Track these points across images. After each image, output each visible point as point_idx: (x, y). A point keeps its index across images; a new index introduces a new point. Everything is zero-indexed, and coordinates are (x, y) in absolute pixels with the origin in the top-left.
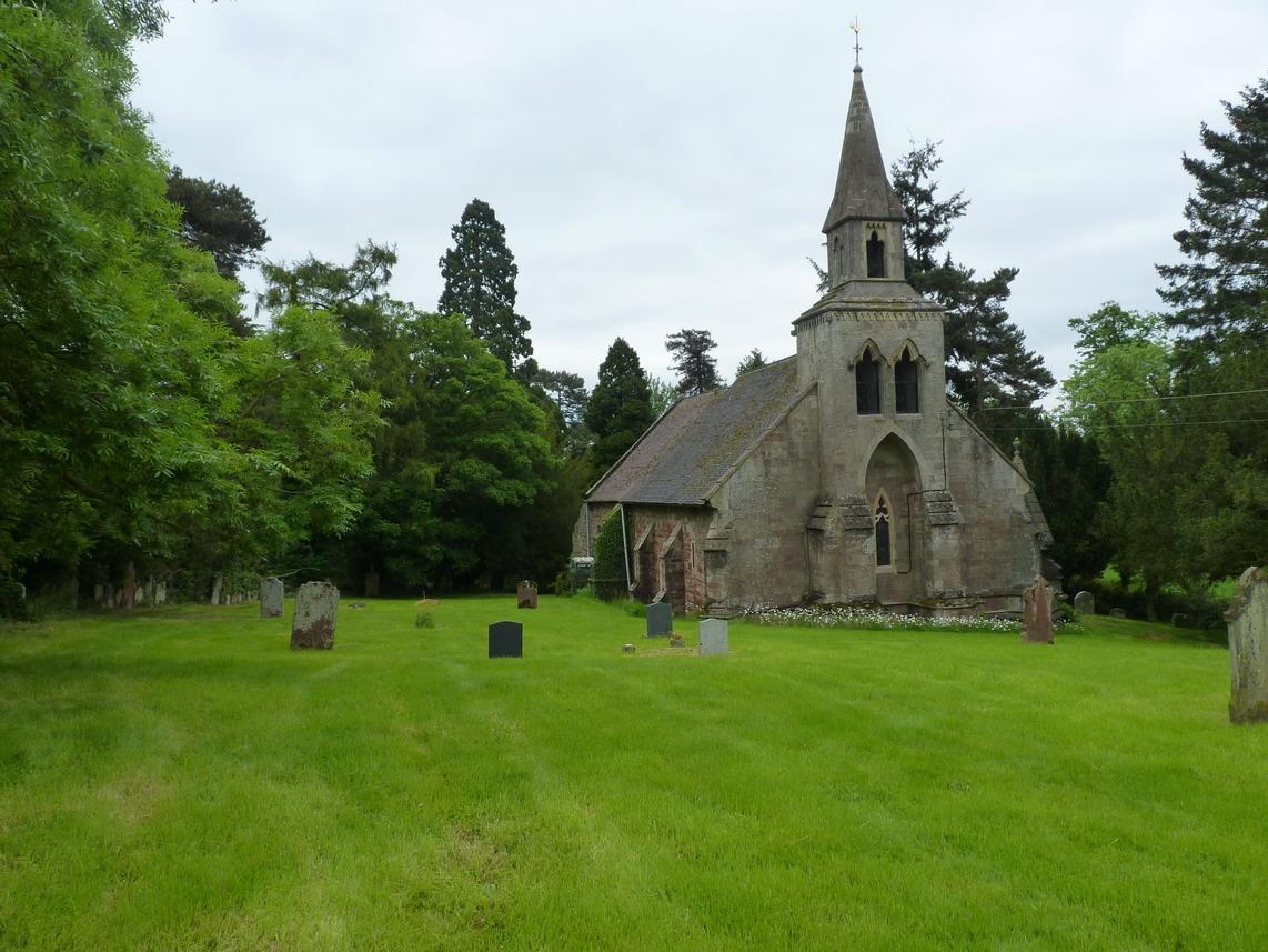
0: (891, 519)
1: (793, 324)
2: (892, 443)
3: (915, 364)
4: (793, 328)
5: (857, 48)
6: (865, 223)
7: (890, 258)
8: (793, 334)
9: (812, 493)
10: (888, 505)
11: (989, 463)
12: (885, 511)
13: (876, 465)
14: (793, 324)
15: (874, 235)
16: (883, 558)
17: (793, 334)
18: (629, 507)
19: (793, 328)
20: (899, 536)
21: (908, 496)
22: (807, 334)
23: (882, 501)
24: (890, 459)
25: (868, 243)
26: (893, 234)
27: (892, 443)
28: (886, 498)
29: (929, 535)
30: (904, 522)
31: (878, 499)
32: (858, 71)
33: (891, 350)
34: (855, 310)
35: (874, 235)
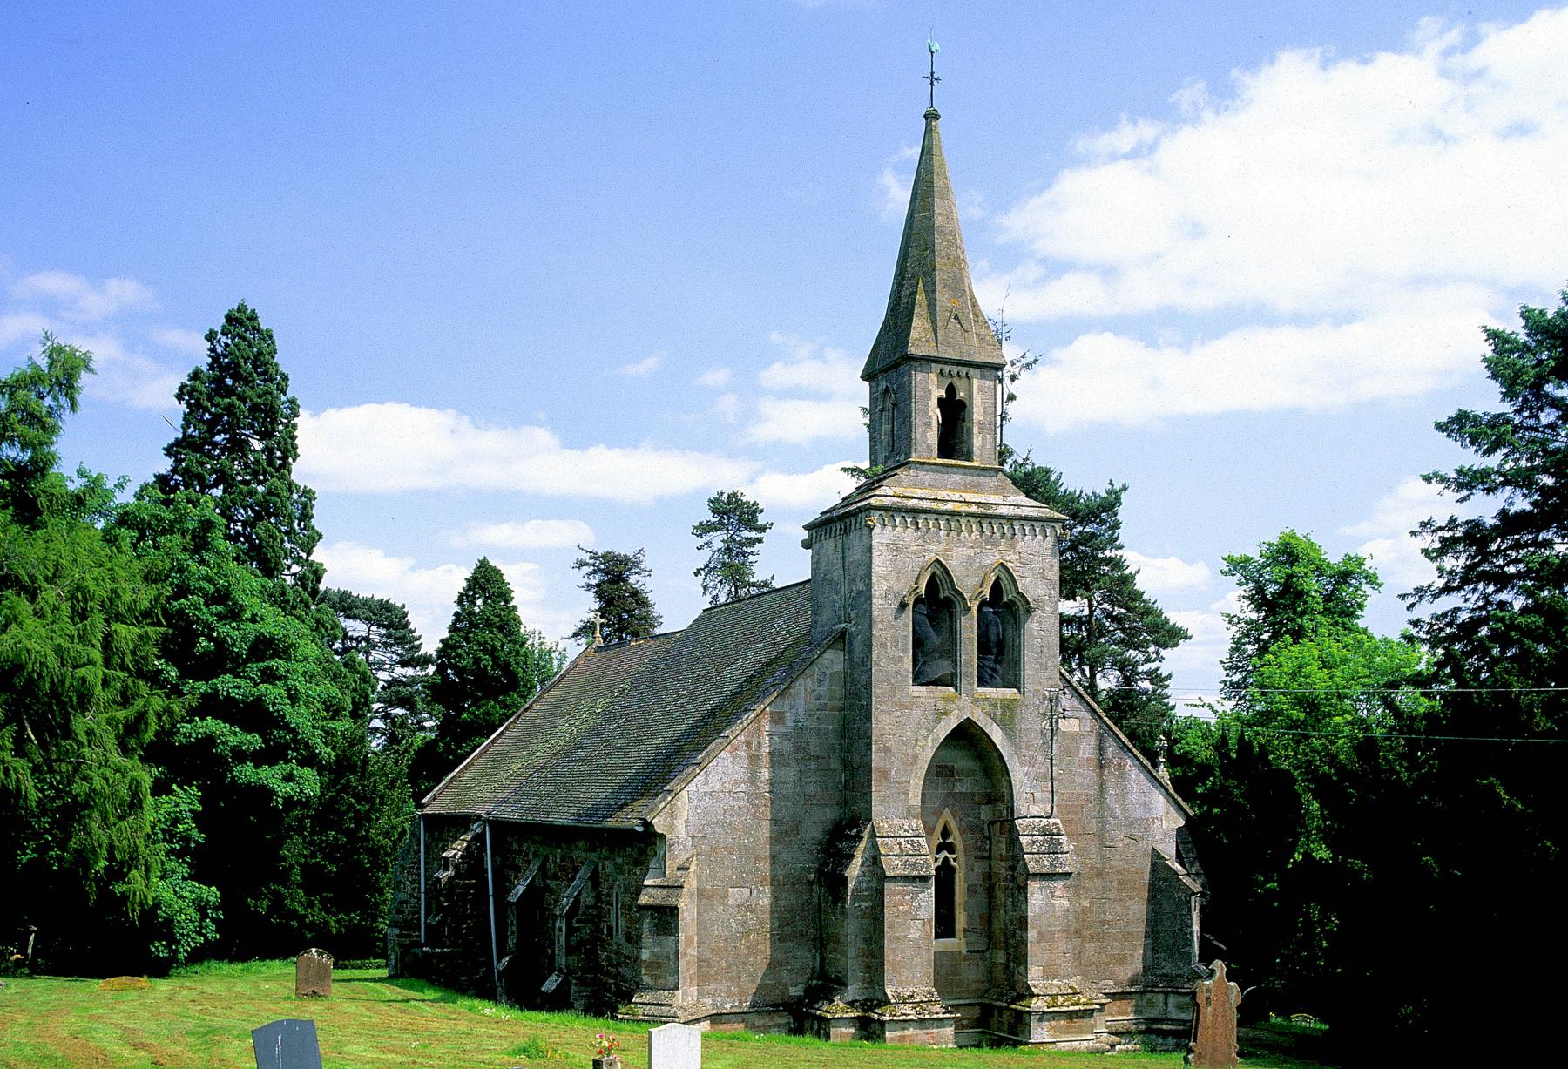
0: (958, 861)
1: (805, 527)
2: (966, 737)
3: (1011, 605)
4: (805, 535)
5: (932, 79)
6: (936, 367)
7: (975, 430)
8: (807, 545)
9: (830, 814)
10: (956, 838)
11: (1122, 774)
12: (950, 848)
13: (939, 771)
14: (805, 527)
15: (951, 390)
16: (944, 925)
17: (807, 545)
18: (503, 830)
19: (805, 535)
20: (971, 890)
21: (992, 823)
22: (829, 546)
23: (946, 833)
24: (962, 761)
25: (940, 401)
26: (981, 390)
27: (966, 737)
28: (953, 826)
29: (1023, 889)
30: (980, 867)
31: (939, 829)
32: (931, 117)
33: (976, 580)
34: (915, 512)
35: (951, 390)
